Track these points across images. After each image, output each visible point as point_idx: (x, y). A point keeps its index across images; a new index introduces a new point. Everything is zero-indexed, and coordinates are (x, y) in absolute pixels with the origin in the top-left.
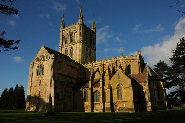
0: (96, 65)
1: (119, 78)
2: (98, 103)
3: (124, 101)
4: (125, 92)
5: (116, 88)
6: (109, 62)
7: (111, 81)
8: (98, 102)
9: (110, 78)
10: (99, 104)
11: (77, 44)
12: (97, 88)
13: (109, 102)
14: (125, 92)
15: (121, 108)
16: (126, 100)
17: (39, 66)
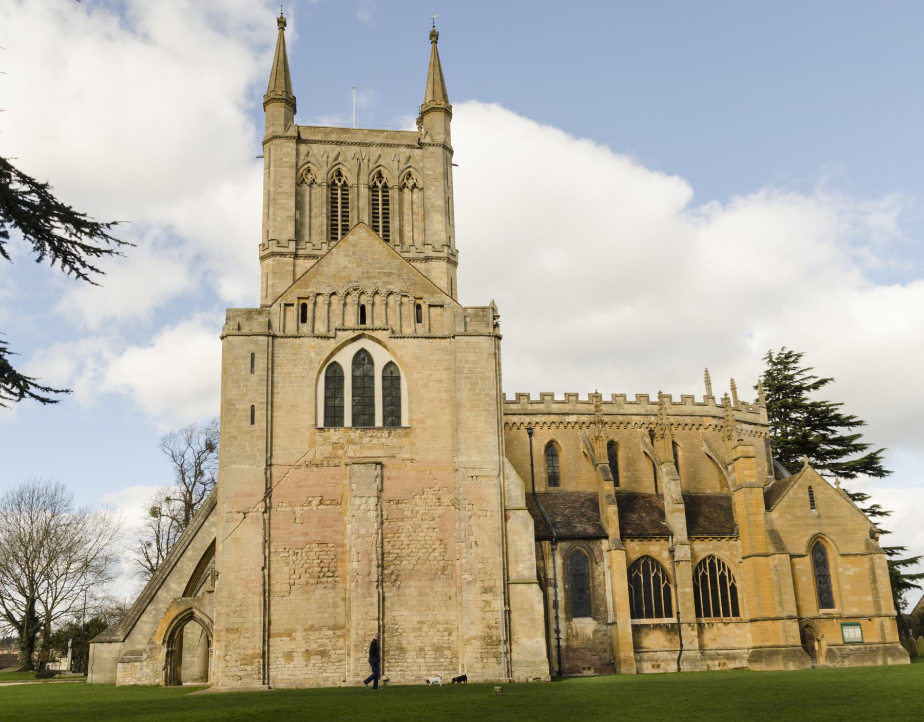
0: (572, 419)
1: (813, 505)
2: (657, 627)
3: (847, 613)
4: (846, 573)
5: (803, 552)
6: (643, 412)
7: (774, 515)
8: (655, 621)
9: (770, 499)
10: (675, 630)
11: (434, 264)
12: (645, 542)
13: (790, 618)
14: (846, 573)
15: (840, 650)
16: (854, 611)
17: (345, 359)
